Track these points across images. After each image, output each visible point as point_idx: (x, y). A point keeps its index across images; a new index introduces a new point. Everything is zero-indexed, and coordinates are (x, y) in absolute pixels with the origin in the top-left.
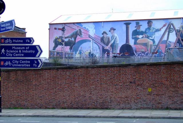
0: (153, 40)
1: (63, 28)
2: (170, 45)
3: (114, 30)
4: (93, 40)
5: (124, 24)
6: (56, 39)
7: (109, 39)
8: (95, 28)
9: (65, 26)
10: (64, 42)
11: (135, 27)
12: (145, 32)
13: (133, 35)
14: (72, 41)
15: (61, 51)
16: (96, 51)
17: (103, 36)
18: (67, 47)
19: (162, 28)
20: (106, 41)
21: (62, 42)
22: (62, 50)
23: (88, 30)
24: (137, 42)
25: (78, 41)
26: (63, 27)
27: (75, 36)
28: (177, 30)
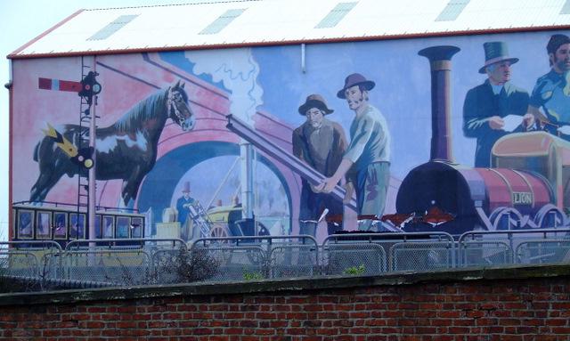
1: (84, 82)
3: (368, 86)
4: (252, 142)
5: (422, 53)
6: (49, 141)
7: (336, 135)
8: (262, 80)
9: (99, 69)
10: (94, 156)
11: (482, 71)
12: (538, 99)
13: (467, 117)
14: (136, 148)
15: (79, 205)
16: (266, 204)
17: (302, 120)
18: (112, 182)
20: (322, 148)
21: (81, 159)
22: (83, 200)
23: (220, 91)
24: (494, 151)
25: (171, 148)
26: (86, 74)
27: (153, 123)
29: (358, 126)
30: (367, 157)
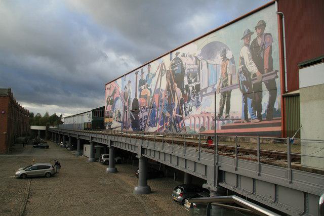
0: (150, 90)
2: (162, 94)
30: (129, 99)
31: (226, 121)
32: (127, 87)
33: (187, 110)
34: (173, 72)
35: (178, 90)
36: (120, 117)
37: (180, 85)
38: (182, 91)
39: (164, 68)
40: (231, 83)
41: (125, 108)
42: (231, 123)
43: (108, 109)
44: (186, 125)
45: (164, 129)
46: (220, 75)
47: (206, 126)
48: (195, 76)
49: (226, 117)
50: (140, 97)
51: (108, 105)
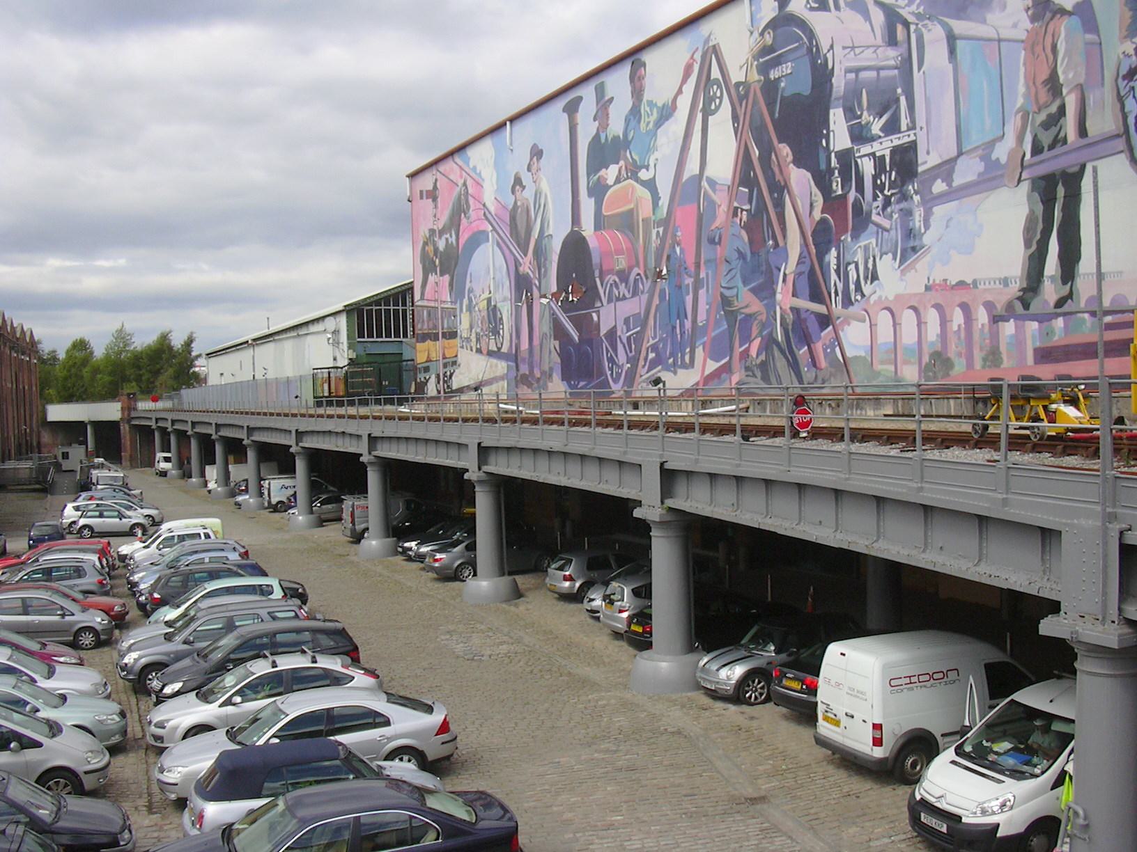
0: (651, 185)
2: (712, 205)
13: (588, 175)
19: (680, 91)
28: (738, 85)
29: (538, 194)
31: (1059, 322)
32: (526, 179)
33: (853, 275)
34: (770, 88)
35: (799, 179)
36: (496, 332)
37: (808, 145)
38: (822, 180)
39: (716, 73)
40: (1083, 132)
41: (522, 285)
42: (1087, 330)
43: (433, 293)
44: (849, 354)
45: (736, 378)
46: (1021, 89)
47: (952, 352)
48: (886, 105)
49: (1060, 303)
50: (598, 226)
51: (432, 278)
